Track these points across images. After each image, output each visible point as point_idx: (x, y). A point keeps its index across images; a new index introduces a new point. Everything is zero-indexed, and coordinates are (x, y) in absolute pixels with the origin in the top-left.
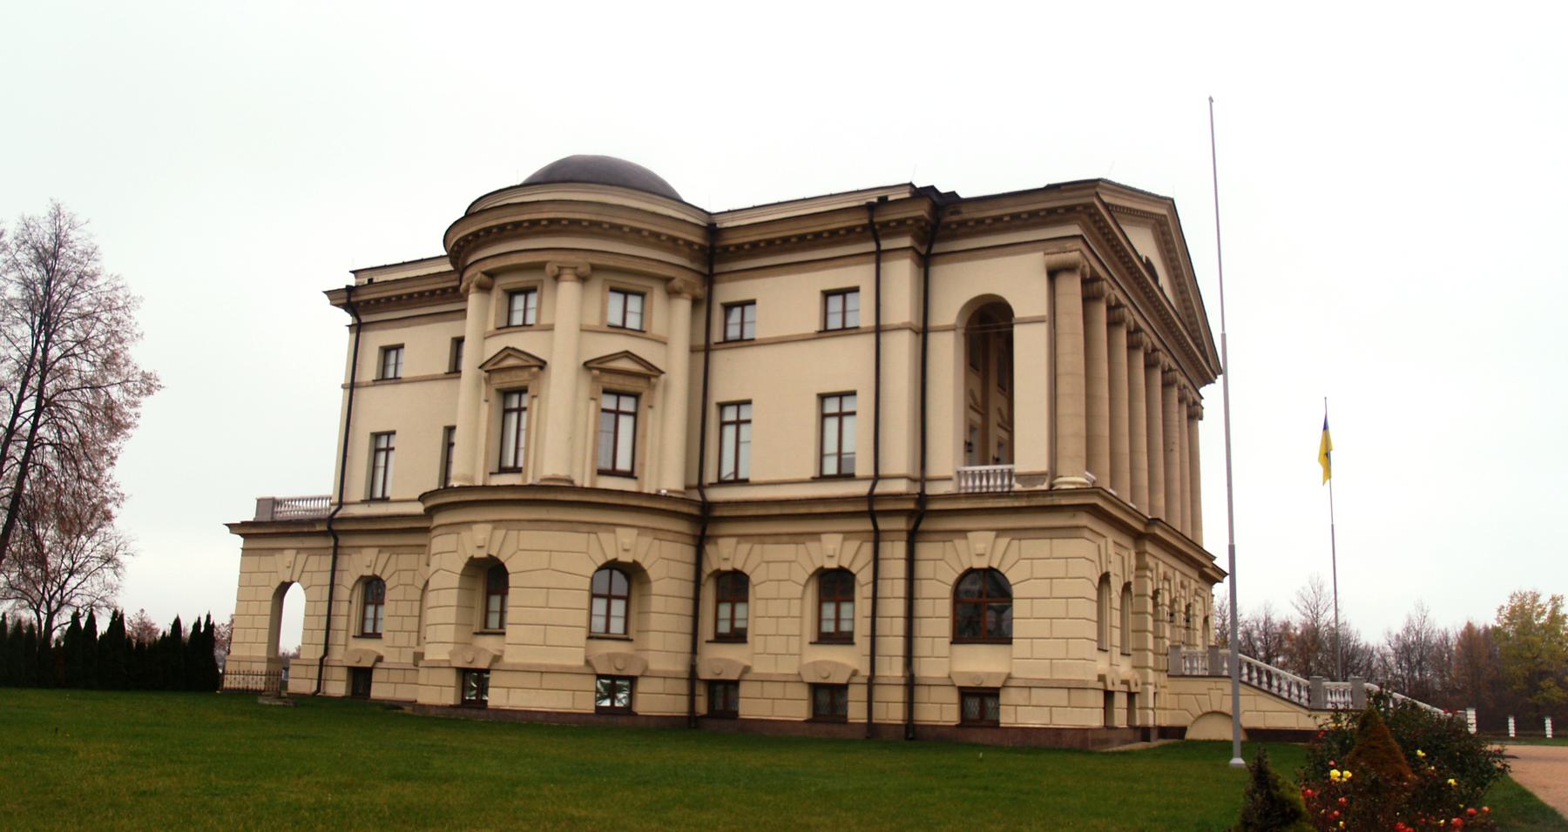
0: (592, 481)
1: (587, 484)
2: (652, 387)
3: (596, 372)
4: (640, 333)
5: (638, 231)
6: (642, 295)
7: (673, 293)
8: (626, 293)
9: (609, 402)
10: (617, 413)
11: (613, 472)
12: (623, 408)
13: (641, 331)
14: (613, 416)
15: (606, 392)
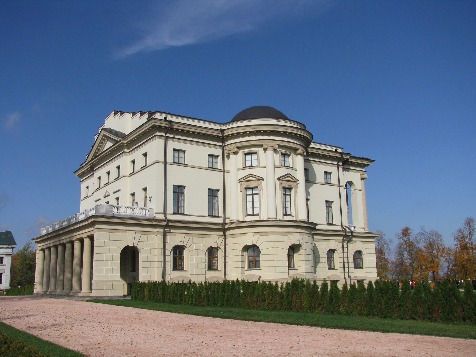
0: (244, 218)
1: (241, 220)
2: (261, 183)
3: (241, 182)
4: (256, 167)
5: (246, 132)
6: (256, 153)
7: (265, 150)
8: (251, 154)
9: (249, 192)
10: (253, 195)
11: (253, 215)
12: (253, 193)
13: (257, 166)
14: (251, 196)
15: (246, 189)
